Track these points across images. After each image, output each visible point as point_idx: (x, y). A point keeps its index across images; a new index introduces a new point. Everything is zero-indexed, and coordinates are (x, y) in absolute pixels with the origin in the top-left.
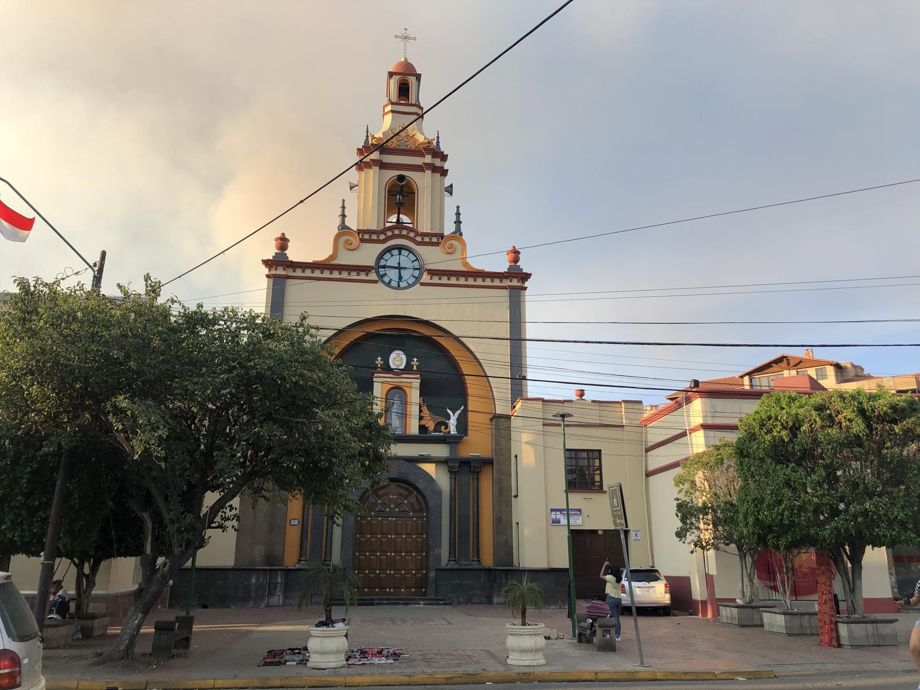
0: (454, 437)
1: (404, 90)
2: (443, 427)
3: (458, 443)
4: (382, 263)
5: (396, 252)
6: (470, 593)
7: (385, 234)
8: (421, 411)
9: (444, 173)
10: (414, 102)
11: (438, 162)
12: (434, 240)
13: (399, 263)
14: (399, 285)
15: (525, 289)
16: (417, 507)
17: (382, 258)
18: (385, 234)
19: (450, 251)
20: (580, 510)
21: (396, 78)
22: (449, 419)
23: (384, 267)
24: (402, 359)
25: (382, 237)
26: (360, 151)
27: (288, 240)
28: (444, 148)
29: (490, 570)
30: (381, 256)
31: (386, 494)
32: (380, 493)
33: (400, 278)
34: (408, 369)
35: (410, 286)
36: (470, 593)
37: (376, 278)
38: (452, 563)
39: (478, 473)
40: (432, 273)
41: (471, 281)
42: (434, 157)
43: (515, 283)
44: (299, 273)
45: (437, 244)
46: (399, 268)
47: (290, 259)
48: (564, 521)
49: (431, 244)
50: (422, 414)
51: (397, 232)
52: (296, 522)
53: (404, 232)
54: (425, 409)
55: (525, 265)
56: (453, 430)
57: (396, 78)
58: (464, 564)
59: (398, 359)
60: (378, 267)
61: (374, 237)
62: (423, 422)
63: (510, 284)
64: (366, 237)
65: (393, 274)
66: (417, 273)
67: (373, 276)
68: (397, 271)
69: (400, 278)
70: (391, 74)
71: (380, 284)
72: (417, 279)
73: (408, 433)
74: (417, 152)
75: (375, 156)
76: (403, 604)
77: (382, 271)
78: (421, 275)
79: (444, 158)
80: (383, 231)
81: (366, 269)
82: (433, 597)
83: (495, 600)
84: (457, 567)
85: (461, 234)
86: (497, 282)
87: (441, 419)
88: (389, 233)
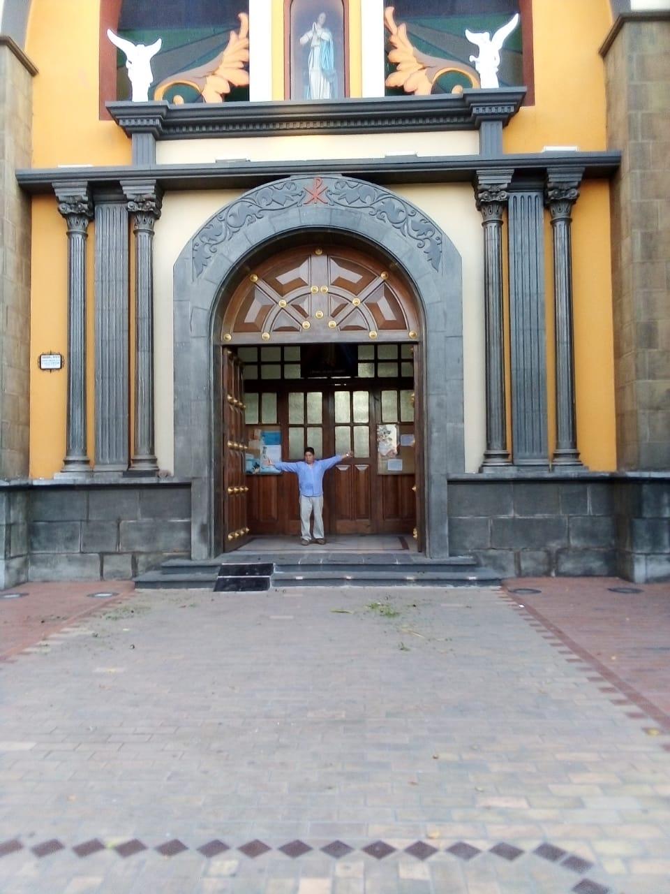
0: (488, 98)
3: (506, 120)
6: (554, 545)
8: (389, 47)
16: (388, 314)
29: (610, 482)
31: (299, 283)
32: (284, 278)
36: (554, 545)
38: (498, 462)
39: (573, 202)
50: (394, 56)
52: (54, 362)
54: (400, 34)
58: (533, 464)
62: (396, 80)
76: (355, 581)
82: (445, 557)
83: (641, 570)
84: (511, 473)
87: (445, 66)
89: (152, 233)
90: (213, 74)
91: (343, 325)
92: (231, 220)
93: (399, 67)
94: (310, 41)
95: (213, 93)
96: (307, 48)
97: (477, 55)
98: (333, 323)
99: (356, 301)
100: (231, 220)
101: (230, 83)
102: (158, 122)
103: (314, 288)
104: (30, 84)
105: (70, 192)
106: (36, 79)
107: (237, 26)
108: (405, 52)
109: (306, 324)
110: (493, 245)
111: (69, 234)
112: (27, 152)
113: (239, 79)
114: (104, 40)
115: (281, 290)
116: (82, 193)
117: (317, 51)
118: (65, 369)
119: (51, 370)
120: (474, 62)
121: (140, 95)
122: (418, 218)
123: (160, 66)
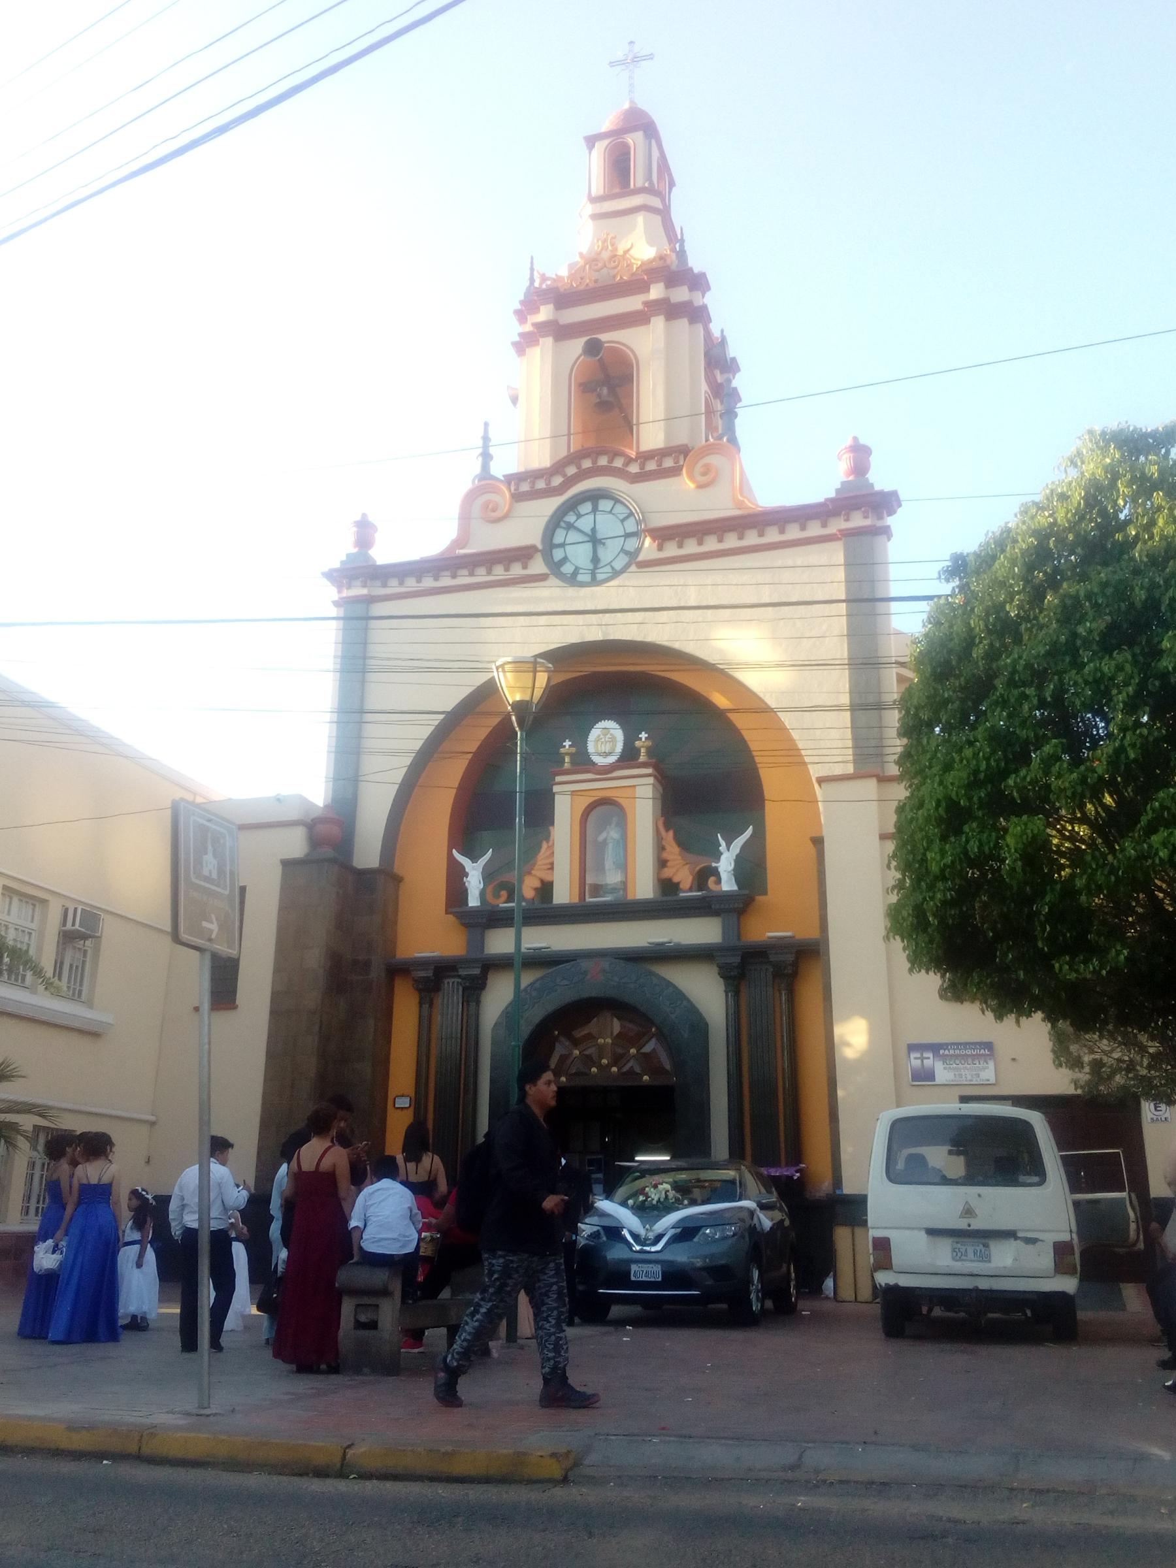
0: (729, 896)
1: (619, 166)
2: (712, 879)
4: (559, 538)
5: (586, 507)
7: (564, 475)
8: (660, 847)
9: (698, 315)
10: (639, 184)
11: (681, 294)
12: (668, 463)
13: (594, 530)
14: (593, 574)
15: (886, 531)
17: (557, 526)
18: (564, 475)
19: (703, 479)
20: (989, 1046)
21: (600, 146)
22: (717, 856)
23: (563, 545)
24: (613, 740)
25: (557, 481)
26: (521, 315)
27: (374, 528)
28: (696, 263)
30: (556, 522)
31: (590, 1037)
32: (579, 1033)
33: (595, 560)
34: (629, 757)
35: (616, 574)
40: (663, 535)
41: (752, 538)
42: (675, 288)
43: (858, 521)
44: (394, 587)
45: (675, 472)
46: (594, 540)
47: (380, 562)
48: (942, 1074)
49: (662, 473)
50: (665, 855)
51: (587, 464)
52: (404, 1102)
53: (603, 461)
55: (880, 479)
56: (728, 884)
57: (600, 146)
59: (606, 738)
60: (549, 543)
61: (541, 484)
62: (667, 873)
63: (844, 525)
64: (525, 487)
65: (579, 555)
66: (632, 544)
67: (538, 566)
68: (589, 546)
69: (595, 560)
70: (591, 141)
71: (553, 581)
72: (632, 555)
73: (630, 897)
74: (636, 285)
75: (545, 313)
77: (558, 554)
79: (698, 282)
80: (557, 468)
81: (523, 554)
85: (733, 440)
86: (815, 529)
88: (571, 470)
89: (478, 1002)
90: (529, 873)
91: (624, 1070)
92: (534, 994)
93: (669, 864)
94: (605, 840)
95: (529, 887)
96: (605, 842)
97: (718, 859)
98: (614, 1069)
99: (633, 1051)
100: (534, 994)
101: (542, 881)
103: (601, 1041)
104: (397, 889)
105: (422, 974)
106: (401, 885)
107: (547, 837)
108: (673, 851)
109: (594, 1070)
110: (731, 1011)
111: (421, 1004)
112: (391, 943)
113: (547, 878)
114: (450, 855)
115: (576, 1043)
116: (430, 974)
117: (610, 846)
118: (412, 1109)
120: (716, 868)
121: (473, 901)
122: (671, 990)
123: (488, 875)
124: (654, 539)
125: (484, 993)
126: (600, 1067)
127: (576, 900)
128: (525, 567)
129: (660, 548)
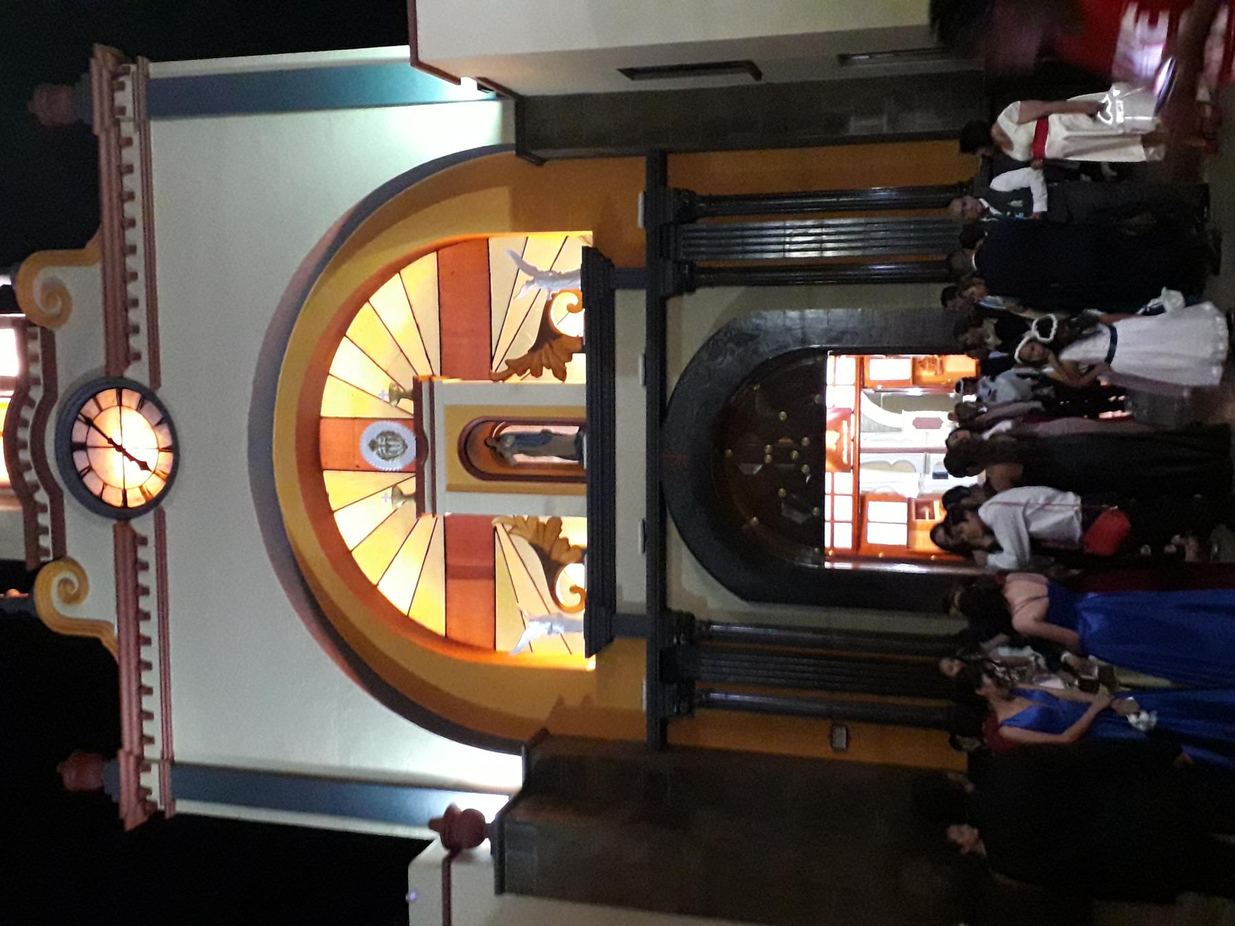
5: (80, 460)
7: (36, 488)
17: (99, 498)
24: (383, 434)
25: (42, 497)
37: (152, 512)
40: (119, 353)
61: (44, 520)
67: (144, 526)
71: (163, 503)
73: (582, 414)
78: (134, 386)
102: (603, 609)
106: (552, 731)
111: (712, 704)
119: (848, 738)
124: (128, 363)
125: (700, 616)
126: (800, 462)
127: (583, 487)
128: (144, 541)
129: (138, 357)
